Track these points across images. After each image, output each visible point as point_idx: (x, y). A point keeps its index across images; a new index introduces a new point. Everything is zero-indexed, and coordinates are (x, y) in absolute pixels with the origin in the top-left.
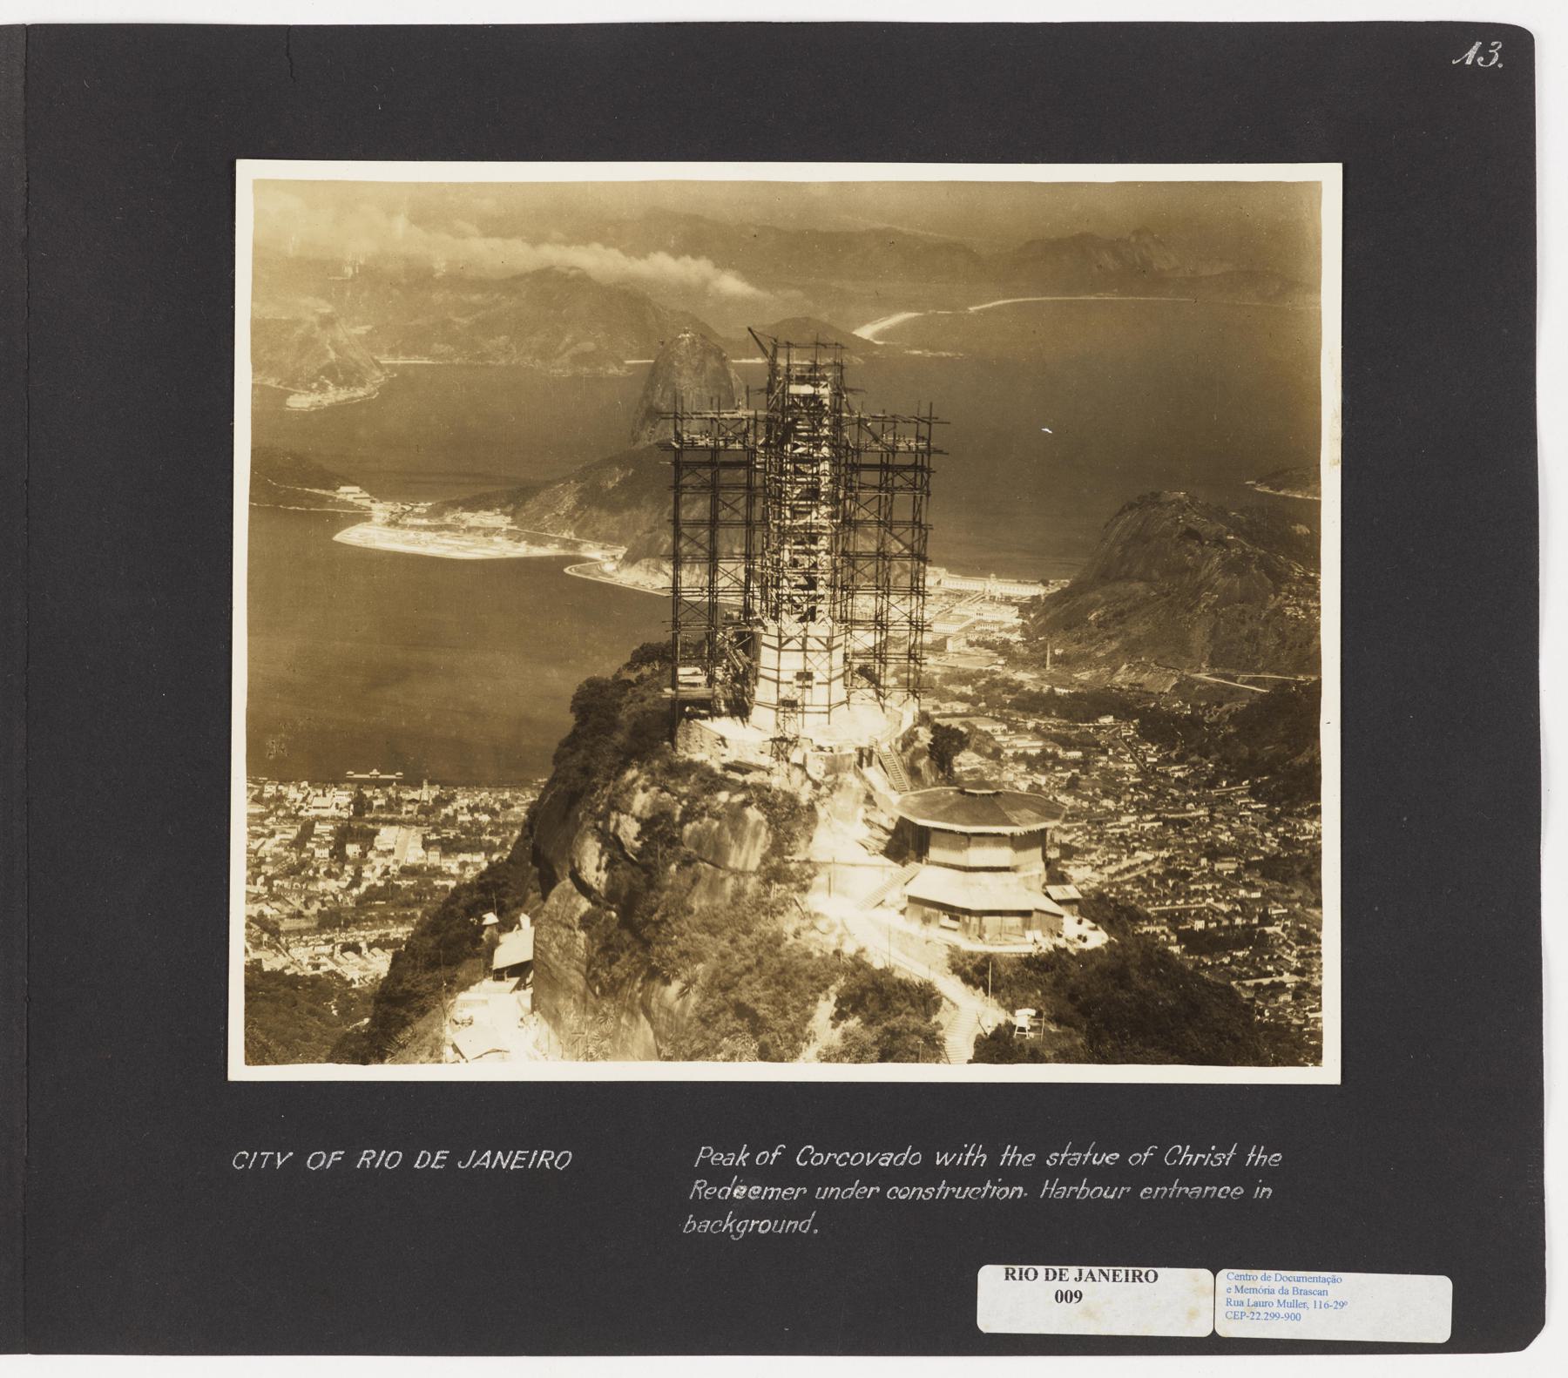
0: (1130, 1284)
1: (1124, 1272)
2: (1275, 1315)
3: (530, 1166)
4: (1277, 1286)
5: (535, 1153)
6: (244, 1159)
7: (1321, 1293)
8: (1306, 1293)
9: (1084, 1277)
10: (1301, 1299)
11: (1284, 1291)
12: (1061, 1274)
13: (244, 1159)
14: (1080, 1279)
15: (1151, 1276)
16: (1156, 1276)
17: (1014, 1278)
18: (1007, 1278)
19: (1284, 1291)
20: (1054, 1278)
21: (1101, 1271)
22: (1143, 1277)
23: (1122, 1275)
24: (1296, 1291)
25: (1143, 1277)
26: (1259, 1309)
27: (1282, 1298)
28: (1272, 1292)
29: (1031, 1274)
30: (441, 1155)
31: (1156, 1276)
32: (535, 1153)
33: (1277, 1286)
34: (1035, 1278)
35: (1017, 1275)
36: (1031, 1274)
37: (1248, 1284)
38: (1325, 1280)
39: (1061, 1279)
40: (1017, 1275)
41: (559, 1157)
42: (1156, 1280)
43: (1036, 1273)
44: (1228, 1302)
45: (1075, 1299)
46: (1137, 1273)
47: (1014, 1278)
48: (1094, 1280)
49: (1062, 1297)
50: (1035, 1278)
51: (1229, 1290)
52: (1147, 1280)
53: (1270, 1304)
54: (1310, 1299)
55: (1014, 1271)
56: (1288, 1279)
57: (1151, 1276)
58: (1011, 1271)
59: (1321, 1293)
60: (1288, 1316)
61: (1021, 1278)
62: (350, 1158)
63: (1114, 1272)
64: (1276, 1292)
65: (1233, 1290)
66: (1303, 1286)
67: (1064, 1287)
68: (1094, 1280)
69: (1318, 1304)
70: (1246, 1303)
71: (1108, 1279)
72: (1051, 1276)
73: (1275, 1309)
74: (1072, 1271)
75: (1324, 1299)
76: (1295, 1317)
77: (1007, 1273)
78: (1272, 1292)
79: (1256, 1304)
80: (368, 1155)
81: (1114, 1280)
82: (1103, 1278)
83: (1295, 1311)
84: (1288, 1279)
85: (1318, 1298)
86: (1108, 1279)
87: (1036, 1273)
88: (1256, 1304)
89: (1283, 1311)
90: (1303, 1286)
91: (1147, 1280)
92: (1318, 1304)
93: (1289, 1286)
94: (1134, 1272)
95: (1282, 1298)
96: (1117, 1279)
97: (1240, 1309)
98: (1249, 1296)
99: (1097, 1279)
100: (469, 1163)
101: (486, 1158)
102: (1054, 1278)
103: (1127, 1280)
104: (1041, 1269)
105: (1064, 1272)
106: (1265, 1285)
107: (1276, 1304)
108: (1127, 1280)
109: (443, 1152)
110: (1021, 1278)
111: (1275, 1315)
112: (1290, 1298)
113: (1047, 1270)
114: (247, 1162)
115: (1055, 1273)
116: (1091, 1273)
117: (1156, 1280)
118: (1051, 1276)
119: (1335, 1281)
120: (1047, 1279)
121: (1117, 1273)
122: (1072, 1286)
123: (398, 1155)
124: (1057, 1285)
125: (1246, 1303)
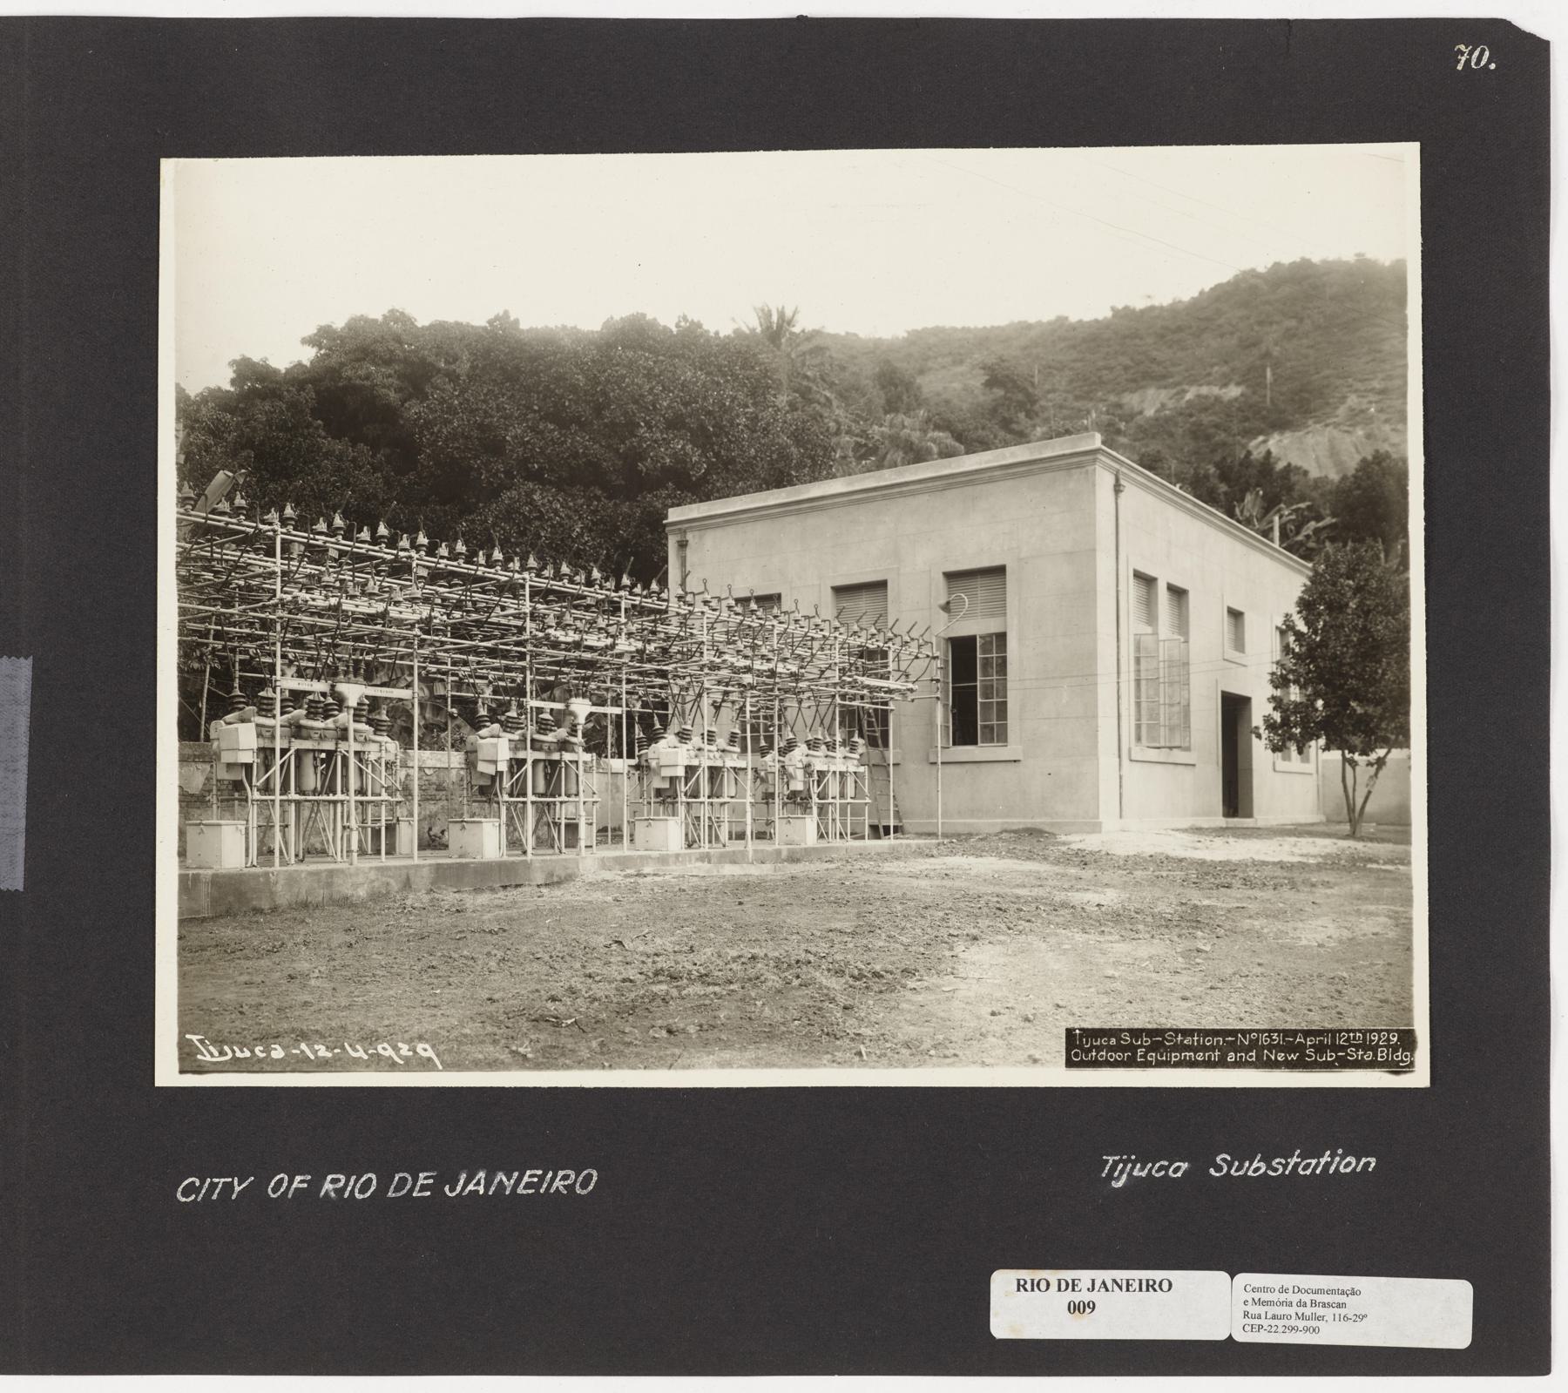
0: (1144, 1294)
1: (1138, 1282)
2: (1293, 1328)
3: (542, 1191)
4: (1295, 1298)
5: (550, 1174)
6: (190, 1190)
7: (1339, 1306)
8: (1324, 1305)
9: (1097, 1287)
10: (1320, 1311)
11: (1301, 1304)
12: (1073, 1285)
13: (190, 1190)
14: (1093, 1289)
15: (1165, 1286)
16: (1170, 1285)
17: (1026, 1290)
18: (1019, 1290)
19: (1301, 1304)
20: (1067, 1289)
21: (1114, 1281)
22: (1156, 1287)
23: (1136, 1285)
24: (1314, 1303)
25: (1156, 1287)
26: (1280, 1323)
27: (1300, 1310)
28: (1291, 1304)
29: (1043, 1285)
30: (531, 1176)
31: (1170, 1285)
32: (550, 1174)
33: (1295, 1298)
34: (1047, 1289)
35: (1028, 1286)
36: (1043, 1285)
37: (1265, 1297)
38: (1343, 1293)
39: (1073, 1290)
40: (1028, 1286)
41: (580, 1178)
42: (1169, 1289)
43: (1048, 1285)
44: (1246, 1315)
45: (1088, 1310)
46: (1151, 1283)
47: (1026, 1290)
48: (1107, 1290)
49: (1076, 1308)
50: (1047, 1289)
51: (1245, 1302)
52: (1161, 1289)
53: (1289, 1317)
54: (1328, 1312)
55: (1026, 1283)
56: (1306, 1291)
57: (1165, 1286)
58: (1022, 1282)
59: (1339, 1306)
60: (1307, 1330)
61: (1033, 1290)
62: (316, 1184)
63: (1128, 1281)
64: (1294, 1304)
65: (1250, 1301)
66: (1320, 1298)
67: (1077, 1297)
68: (1107, 1290)
69: (1337, 1317)
70: (1263, 1316)
71: (1121, 1289)
72: (1063, 1286)
73: (1293, 1322)
74: (1085, 1276)
75: (1343, 1311)
76: (1314, 1330)
77: (1019, 1284)
78: (1291, 1304)
79: (1274, 1317)
80: (334, 1181)
81: (1128, 1290)
82: (1115, 1287)
83: (1314, 1323)
84: (1306, 1291)
85: (1338, 1311)
86: (1121, 1288)
87: (1048, 1285)
88: (1274, 1317)
89: (1301, 1324)
90: (1320, 1298)
91: (1161, 1289)
92: (1337, 1317)
93: (1307, 1298)
94: (1148, 1281)
95: (1300, 1310)
96: (1131, 1289)
97: (1257, 1322)
98: (1266, 1308)
99: (1110, 1289)
100: (459, 1188)
101: (479, 1180)
102: (1067, 1289)
103: (1141, 1290)
104: (1052, 1276)
105: (1076, 1282)
106: (1283, 1297)
107: (1294, 1317)
108: (1141, 1290)
109: (533, 1172)
110: (1033, 1290)
111: (1293, 1328)
112: (1308, 1311)
113: (1059, 1281)
114: (197, 1190)
115: (1067, 1285)
116: (1104, 1283)
117: (1169, 1289)
118: (1063, 1286)
119: (1353, 1292)
120: (1059, 1290)
121: (1131, 1282)
122: (1085, 1296)
123: (591, 1175)
124: (1069, 1296)
125: (1263, 1316)
